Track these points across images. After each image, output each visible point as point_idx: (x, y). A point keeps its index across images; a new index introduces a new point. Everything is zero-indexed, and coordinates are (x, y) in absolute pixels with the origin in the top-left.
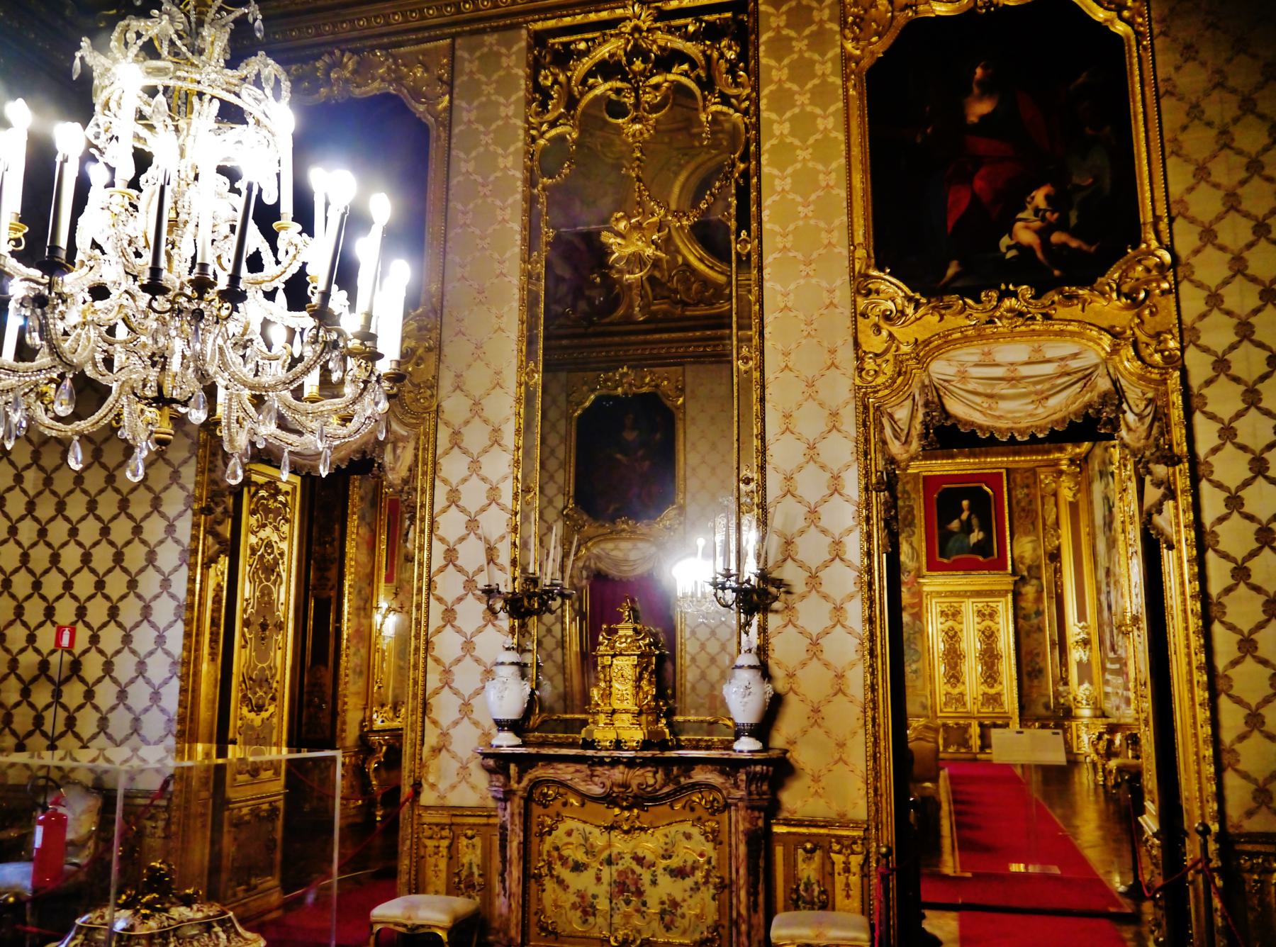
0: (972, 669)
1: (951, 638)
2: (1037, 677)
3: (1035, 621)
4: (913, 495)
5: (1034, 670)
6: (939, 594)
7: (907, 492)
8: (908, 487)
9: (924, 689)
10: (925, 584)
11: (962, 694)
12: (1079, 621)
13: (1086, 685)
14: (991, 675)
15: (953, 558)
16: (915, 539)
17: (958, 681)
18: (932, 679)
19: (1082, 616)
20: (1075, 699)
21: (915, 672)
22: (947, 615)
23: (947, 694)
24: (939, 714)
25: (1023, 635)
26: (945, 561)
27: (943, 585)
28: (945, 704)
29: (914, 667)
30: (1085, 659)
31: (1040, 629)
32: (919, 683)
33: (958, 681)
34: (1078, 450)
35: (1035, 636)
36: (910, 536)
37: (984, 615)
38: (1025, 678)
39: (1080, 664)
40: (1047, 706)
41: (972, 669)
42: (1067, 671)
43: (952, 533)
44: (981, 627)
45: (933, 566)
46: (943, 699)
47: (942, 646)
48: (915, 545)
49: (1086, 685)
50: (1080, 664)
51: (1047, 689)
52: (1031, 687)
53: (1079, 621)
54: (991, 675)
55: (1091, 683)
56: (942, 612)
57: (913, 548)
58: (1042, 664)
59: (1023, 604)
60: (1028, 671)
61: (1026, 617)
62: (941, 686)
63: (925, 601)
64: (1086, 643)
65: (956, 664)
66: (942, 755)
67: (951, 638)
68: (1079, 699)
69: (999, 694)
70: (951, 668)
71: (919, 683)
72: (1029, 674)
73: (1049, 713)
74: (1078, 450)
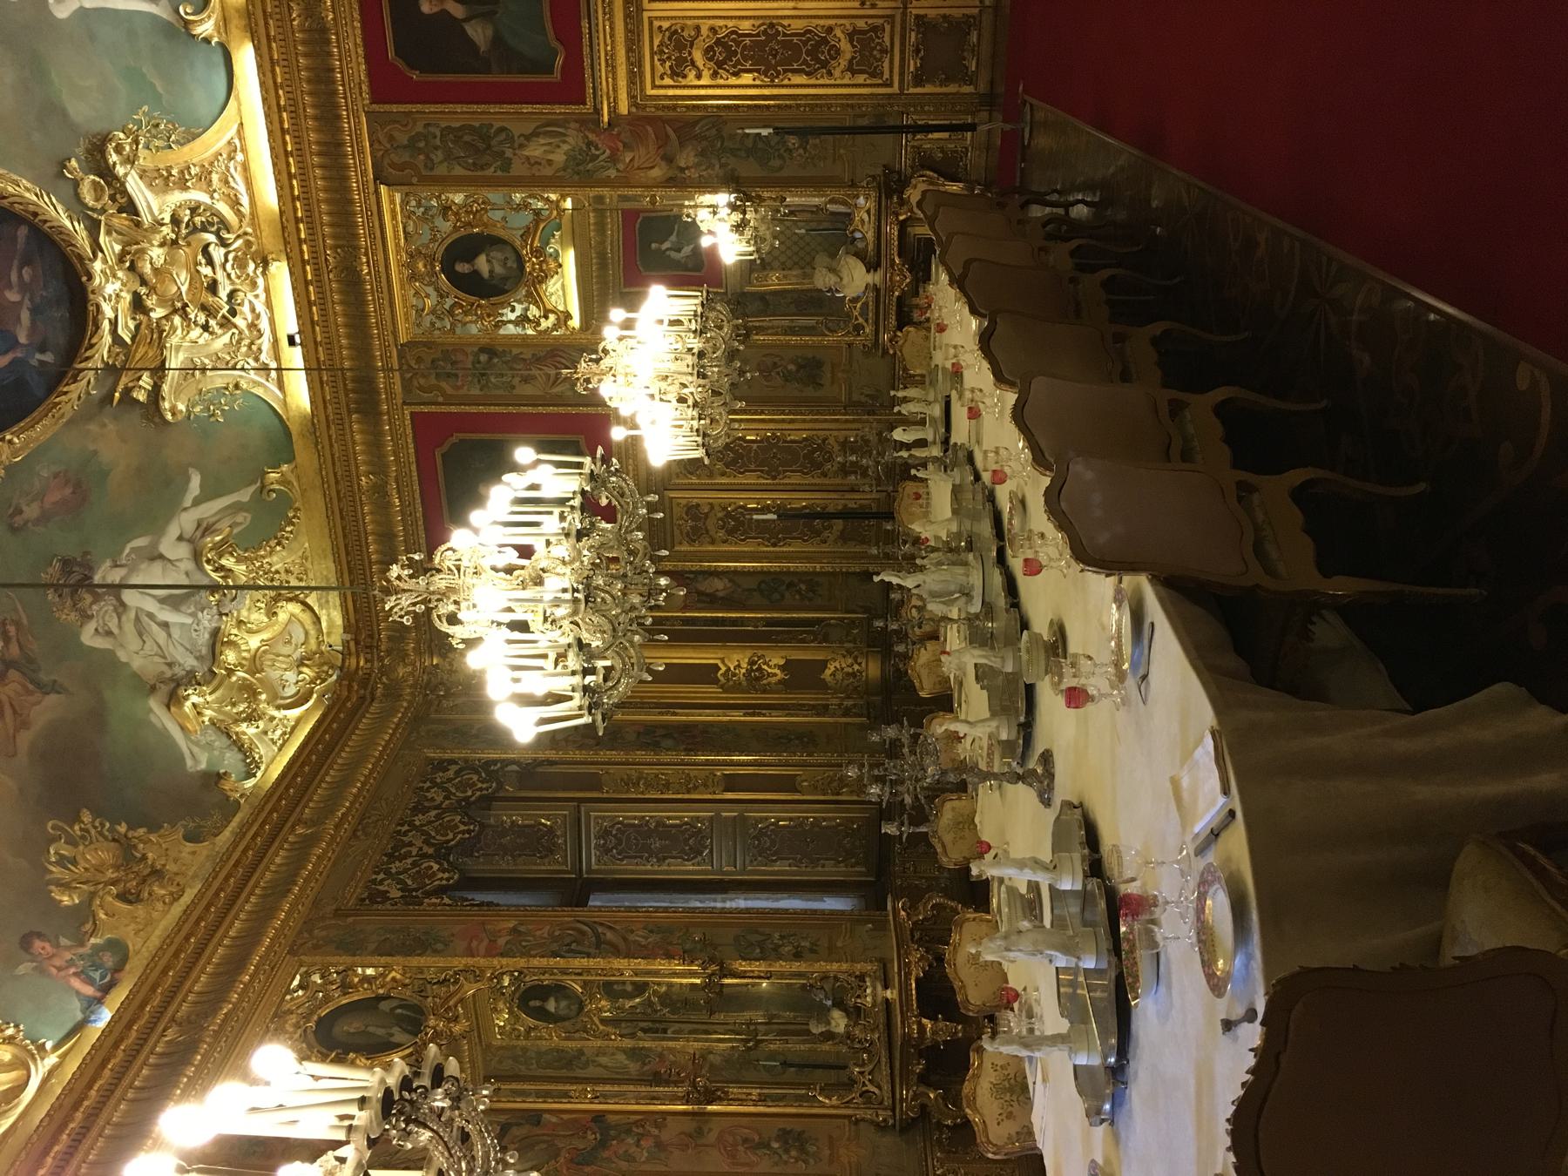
1: (731, 54)
4: (419, 128)
6: (635, 77)
7: (413, 140)
8: (403, 139)
10: (613, 110)
11: (851, 35)
15: (555, 44)
16: (517, 129)
17: (824, 41)
22: (681, 62)
23: (852, 69)
24: (896, 89)
26: (559, 61)
27: (612, 67)
28: (873, 75)
36: (510, 139)
43: (497, 41)
45: (572, 87)
46: (860, 79)
47: (747, 78)
48: (529, 128)
56: (675, 74)
57: (535, 134)
63: (650, 111)
66: (983, 87)
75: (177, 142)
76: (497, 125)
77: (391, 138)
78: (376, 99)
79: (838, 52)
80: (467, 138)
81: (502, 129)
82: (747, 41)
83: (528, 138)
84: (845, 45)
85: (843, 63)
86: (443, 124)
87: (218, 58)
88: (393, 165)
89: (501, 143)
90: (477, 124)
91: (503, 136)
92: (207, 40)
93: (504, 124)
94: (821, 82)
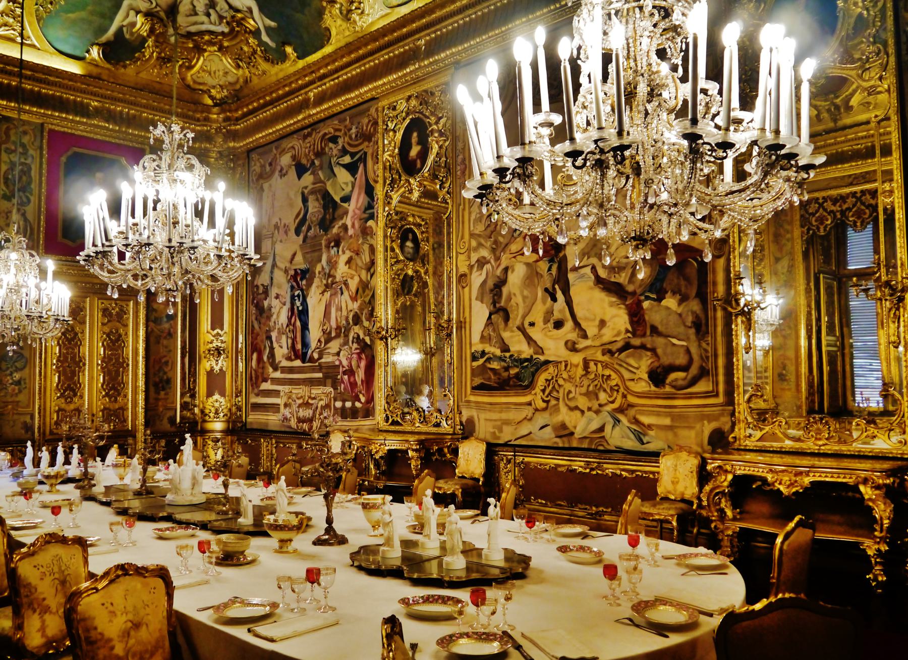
0: (92, 381)
1: (70, 341)
2: (164, 389)
3: (167, 326)
4: (31, 152)
5: (161, 381)
8: (26, 140)
9: (28, 406)
12: (213, 329)
13: (217, 396)
14: (114, 384)
18: (43, 391)
19: (217, 322)
20: (202, 412)
21: (18, 383)
23: (60, 410)
25: (152, 339)
28: (57, 423)
29: (17, 376)
30: (217, 368)
31: (171, 335)
32: (21, 398)
33: (75, 395)
34: (231, 144)
35: (165, 342)
37: (111, 315)
38: (152, 389)
39: (210, 373)
40: (172, 420)
41: (92, 381)
42: (195, 381)
44: (106, 329)
48: (30, 217)
49: (217, 396)
50: (210, 373)
51: (174, 402)
52: (157, 400)
53: (213, 329)
54: (114, 384)
55: (223, 394)
57: (26, 220)
58: (170, 375)
59: (155, 306)
60: (157, 382)
61: (157, 321)
62: (53, 401)
64: (218, 352)
65: (73, 373)
67: (70, 341)
68: (207, 411)
69: (123, 409)
70: (67, 378)
71: (21, 398)
72: (156, 385)
73: (173, 429)
74: (231, 144)
75: (37, 10)
76: (32, 198)
77: (25, 133)
78: (51, 132)
79: (70, 402)
80: (24, 178)
81: (29, 201)
82: (76, 351)
83: (24, 215)
84: (72, 407)
85: (63, 406)
86: (33, 167)
87: (77, 53)
88: (8, 129)
89: (21, 198)
90: (33, 186)
91: (25, 200)
92: (88, 51)
93: (32, 204)
94: (53, 394)
